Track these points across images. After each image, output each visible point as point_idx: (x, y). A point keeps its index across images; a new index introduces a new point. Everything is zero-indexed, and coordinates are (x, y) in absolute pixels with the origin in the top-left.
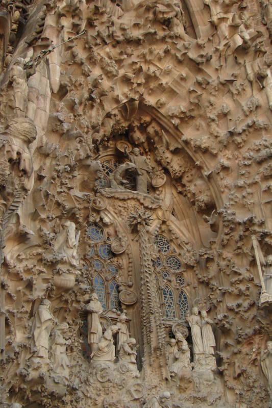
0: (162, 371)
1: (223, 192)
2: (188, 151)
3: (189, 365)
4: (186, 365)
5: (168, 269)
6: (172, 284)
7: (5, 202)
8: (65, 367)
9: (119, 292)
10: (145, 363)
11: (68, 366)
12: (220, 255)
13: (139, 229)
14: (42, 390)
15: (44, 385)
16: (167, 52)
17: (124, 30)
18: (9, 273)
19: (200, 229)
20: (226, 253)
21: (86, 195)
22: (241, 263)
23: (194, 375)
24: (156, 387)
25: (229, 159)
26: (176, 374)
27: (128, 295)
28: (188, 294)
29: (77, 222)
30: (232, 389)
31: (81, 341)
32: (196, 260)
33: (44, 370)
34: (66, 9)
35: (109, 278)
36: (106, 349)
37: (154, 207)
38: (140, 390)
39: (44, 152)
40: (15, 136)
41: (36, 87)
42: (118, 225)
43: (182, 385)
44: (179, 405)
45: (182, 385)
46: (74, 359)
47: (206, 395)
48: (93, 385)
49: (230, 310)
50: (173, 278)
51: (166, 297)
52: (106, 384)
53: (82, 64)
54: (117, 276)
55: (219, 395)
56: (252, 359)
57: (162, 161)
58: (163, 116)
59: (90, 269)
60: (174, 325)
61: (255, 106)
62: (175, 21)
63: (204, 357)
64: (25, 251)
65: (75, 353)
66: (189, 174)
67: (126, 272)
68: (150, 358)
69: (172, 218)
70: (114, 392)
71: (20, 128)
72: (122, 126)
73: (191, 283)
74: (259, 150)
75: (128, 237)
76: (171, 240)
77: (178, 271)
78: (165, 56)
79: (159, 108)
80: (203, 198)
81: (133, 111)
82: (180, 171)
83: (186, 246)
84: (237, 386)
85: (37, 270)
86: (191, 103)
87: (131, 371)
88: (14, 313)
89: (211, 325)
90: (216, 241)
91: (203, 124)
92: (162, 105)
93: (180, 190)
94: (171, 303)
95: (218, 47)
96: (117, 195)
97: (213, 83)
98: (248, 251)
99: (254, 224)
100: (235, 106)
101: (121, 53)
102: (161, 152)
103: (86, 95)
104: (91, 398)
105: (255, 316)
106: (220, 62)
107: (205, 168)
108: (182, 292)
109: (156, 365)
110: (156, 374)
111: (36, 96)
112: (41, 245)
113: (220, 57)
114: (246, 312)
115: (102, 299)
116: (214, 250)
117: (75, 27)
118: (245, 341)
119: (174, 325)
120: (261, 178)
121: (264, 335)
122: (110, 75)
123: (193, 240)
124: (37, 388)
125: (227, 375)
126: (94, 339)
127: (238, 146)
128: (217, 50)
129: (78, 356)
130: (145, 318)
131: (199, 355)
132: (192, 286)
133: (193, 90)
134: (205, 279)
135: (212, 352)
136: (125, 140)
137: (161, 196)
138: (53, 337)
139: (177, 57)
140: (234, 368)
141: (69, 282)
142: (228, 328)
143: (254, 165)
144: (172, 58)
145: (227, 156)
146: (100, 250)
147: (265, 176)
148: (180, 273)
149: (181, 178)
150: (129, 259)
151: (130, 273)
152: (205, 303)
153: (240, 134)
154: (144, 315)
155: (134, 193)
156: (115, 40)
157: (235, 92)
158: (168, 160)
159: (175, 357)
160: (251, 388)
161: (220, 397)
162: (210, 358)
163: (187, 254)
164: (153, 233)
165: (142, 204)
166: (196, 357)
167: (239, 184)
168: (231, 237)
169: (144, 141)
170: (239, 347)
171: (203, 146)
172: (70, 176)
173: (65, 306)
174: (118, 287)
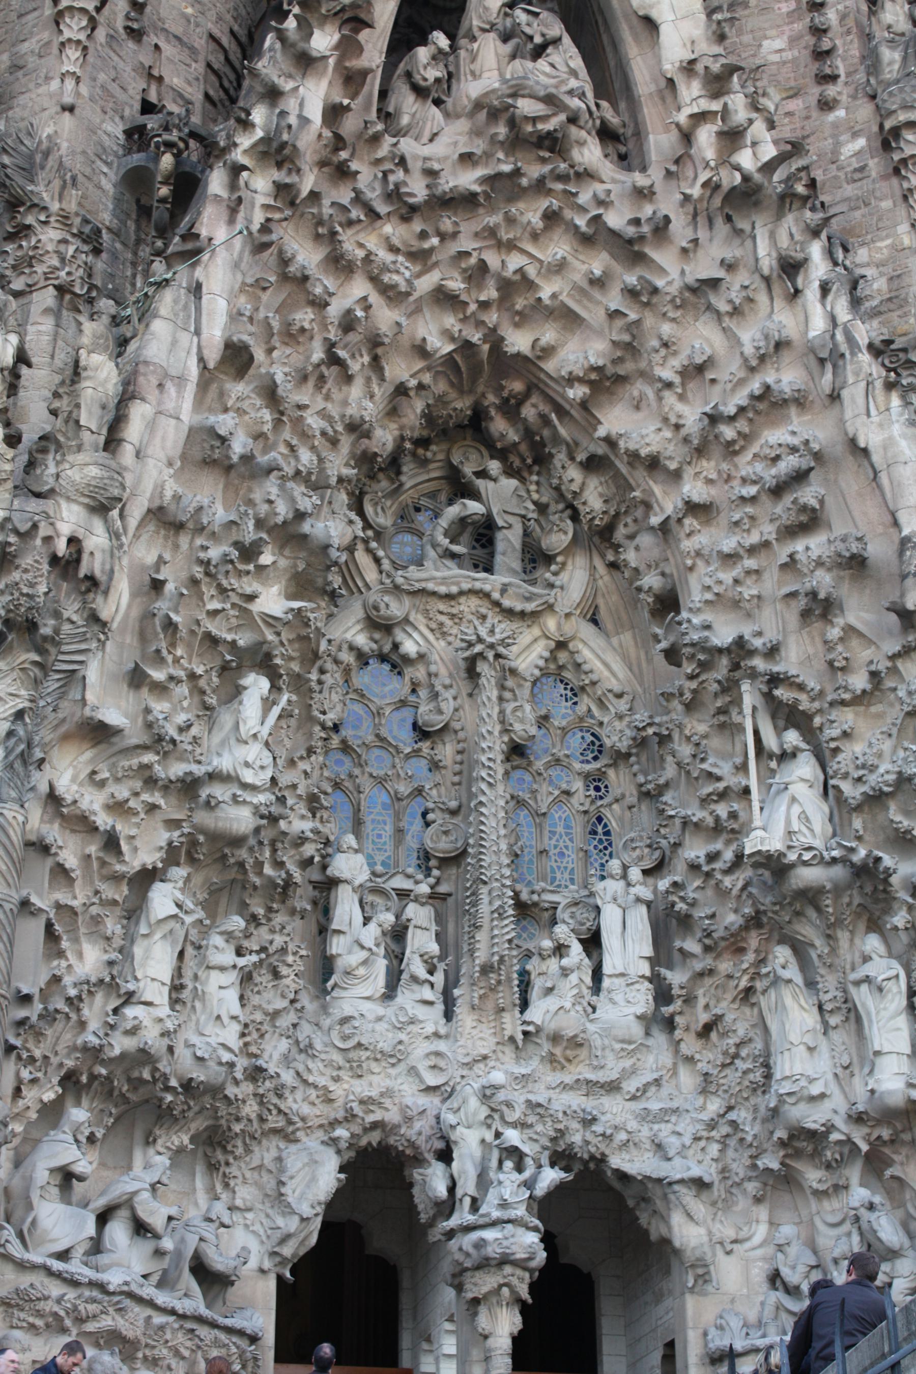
4: (568, 1005)
6: (575, 800)
7: (37, 658)
8: (226, 1020)
9: (428, 824)
11: (234, 1018)
12: (680, 726)
13: (478, 670)
14: (153, 1077)
16: (551, 217)
17: (431, 173)
18: (62, 815)
20: (695, 723)
21: (292, 610)
22: (729, 747)
23: (591, 1027)
24: (485, 1058)
25: (709, 482)
26: (539, 1030)
32: (634, 739)
34: (261, 148)
36: (361, 971)
37: (530, 607)
38: (442, 1064)
39: (171, 519)
40: (68, 499)
41: (156, 360)
42: (437, 658)
43: (558, 1051)
46: (283, 996)
48: (323, 1056)
49: (694, 867)
50: (578, 785)
52: (352, 1055)
53: (306, 278)
60: (564, 902)
61: (772, 343)
62: (575, 132)
64: (114, 759)
66: (629, 520)
69: (587, 630)
70: (376, 1070)
71: (77, 478)
72: (455, 409)
74: (776, 459)
76: (583, 689)
77: (588, 767)
78: (546, 228)
79: (539, 358)
80: (652, 581)
81: (476, 370)
82: (604, 513)
83: (614, 700)
86: (613, 342)
88: (71, 908)
89: (649, 907)
91: (650, 393)
92: (548, 351)
94: (566, 847)
95: (688, 191)
96: (430, 586)
97: (669, 289)
99: (752, 653)
100: (726, 343)
101: (423, 235)
103: (318, 355)
104: (316, 1087)
106: (695, 229)
108: (600, 819)
111: (155, 382)
113: (695, 215)
114: (728, 871)
117: (282, 190)
118: (723, 944)
120: (778, 532)
121: (771, 931)
122: (391, 294)
126: (337, 946)
128: (687, 198)
133: (617, 312)
134: (650, 786)
135: (646, 969)
136: (474, 440)
137: (562, 575)
139: (576, 227)
143: (764, 498)
144: (567, 230)
147: (786, 527)
153: (732, 419)
156: (405, 203)
157: (724, 307)
158: (575, 487)
161: (656, 1080)
162: (637, 986)
163: (618, 725)
164: (527, 675)
165: (497, 604)
166: (606, 983)
169: (517, 439)
172: (251, 567)
173: (240, 877)
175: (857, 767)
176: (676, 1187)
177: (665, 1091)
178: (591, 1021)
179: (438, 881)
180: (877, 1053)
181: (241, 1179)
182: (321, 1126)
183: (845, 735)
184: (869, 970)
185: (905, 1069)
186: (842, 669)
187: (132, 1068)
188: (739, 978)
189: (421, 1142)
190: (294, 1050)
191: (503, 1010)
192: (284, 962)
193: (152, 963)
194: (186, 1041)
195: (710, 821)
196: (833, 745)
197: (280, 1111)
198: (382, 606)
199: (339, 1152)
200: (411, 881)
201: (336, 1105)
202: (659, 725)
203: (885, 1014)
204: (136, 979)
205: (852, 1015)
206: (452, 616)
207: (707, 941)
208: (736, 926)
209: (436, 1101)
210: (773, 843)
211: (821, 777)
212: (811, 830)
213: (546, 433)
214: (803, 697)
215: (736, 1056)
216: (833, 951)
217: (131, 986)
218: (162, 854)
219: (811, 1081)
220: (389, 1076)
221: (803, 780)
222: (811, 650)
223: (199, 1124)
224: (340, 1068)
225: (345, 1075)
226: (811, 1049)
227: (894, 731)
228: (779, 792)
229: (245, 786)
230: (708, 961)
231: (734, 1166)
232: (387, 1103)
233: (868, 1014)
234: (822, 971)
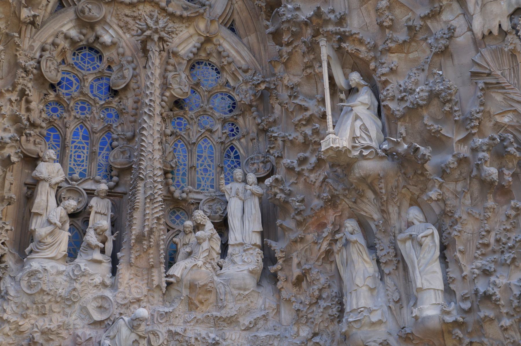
4: (200, 263)
6: (215, 136)
20: (291, 77)
24: (139, 300)
26: (179, 281)
28: (242, 151)
30: (288, 301)
31: (8, 227)
35: (98, 126)
36: (49, 240)
37: (185, 14)
38: (106, 305)
42: (124, 45)
44: (179, 330)
45: (193, 298)
47: (236, 313)
49: (290, 169)
52: (38, 298)
54: (114, 125)
55: (263, 313)
56: (322, 251)
63: (242, 250)
68: (131, 253)
69: (225, 32)
83: (244, 75)
84: (298, 296)
87: (91, 275)
89: (260, 198)
94: (209, 166)
99: (327, 22)
104: (9, 322)
108: (232, 148)
109: (142, 263)
110: (143, 280)
114: (311, 171)
115: (83, 161)
142: (282, 200)
146: (92, 87)
148: (232, 117)
161: (264, 316)
162: (251, 251)
163: (244, 87)
165: (163, 10)
166: (230, 250)
175: (401, 92)
177: (270, 324)
178: (218, 276)
179: (117, 184)
180: (420, 290)
183: (392, 71)
184: (412, 231)
186: (390, 27)
188: (321, 244)
191: (152, 267)
195: (301, 139)
196: (383, 78)
198: (87, 10)
201: (25, 335)
202: (269, 82)
205: (401, 265)
206: (134, 18)
207: (298, 218)
208: (319, 207)
209: (101, 331)
211: (376, 103)
212: (369, 137)
214: (363, 49)
215: (320, 298)
216: (386, 222)
219: (371, 311)
220: (66, 315)
221: (363, 104)
226: (371, 290)
227: (426, 67)
228: (346, 113)
230: (299, 233)
232: (64, 333)
233: (412, 262)
234: (378, 236)
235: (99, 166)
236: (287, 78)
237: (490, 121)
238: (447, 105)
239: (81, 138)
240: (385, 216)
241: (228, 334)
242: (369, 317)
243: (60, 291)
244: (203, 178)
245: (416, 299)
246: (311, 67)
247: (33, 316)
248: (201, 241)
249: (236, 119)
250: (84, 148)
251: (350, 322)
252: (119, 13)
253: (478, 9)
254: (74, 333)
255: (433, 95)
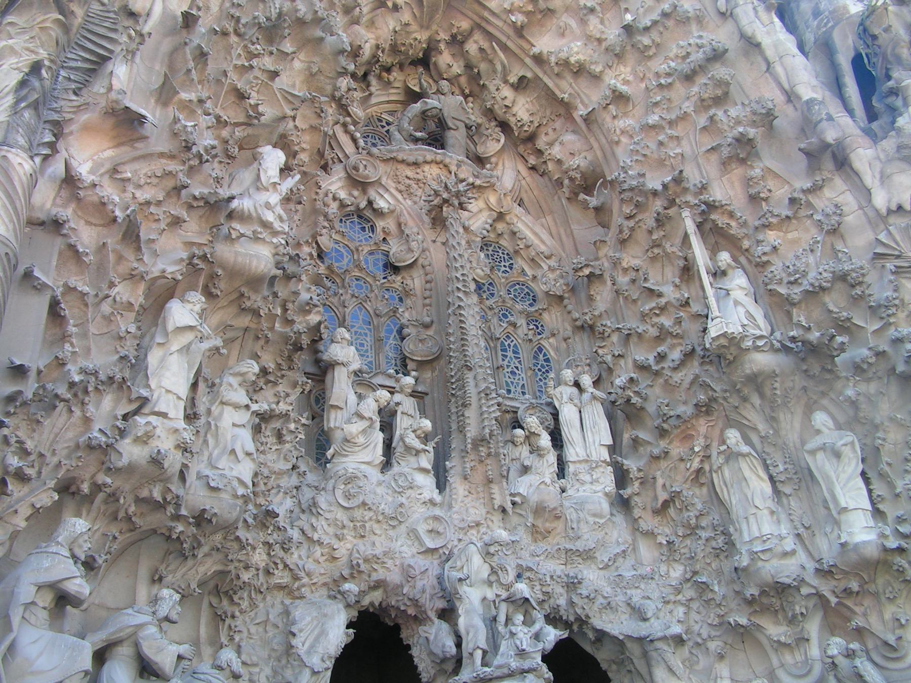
0: (493, 491)
1: (617, 143)
2: (546, 79)
3: (553, 482)
4: (548, 481)
5: (509, 303)
8: (241, 455)
9: (403, 339)
10: (452, 472)
11: (248, 454)
12: (616, 263)
13: (445, 214)
14: (165, 499)
15: (169, 486)
18: (79, 200)
19: (575, 232)
20: (630, 259)
23: (566, 504)
24: (478, 524)
27: (421, 341)
28: (552, 353)
29: (291, 154)
30: (650, 535)
31: (304, 421)
33: (165, 443)
36: (361, 440)
38: (441, 529)
42: (405, 212)
43: (539, 523)
44: (531, 565)
45: (540, 525)
49: (643, 368)
50: (522, 322)
51: (506, 356)
52: (358, 514)
54: (401, 310)
56: (692, 469)
57: (496, 107)
58: (493, 14)
59: (341, 291)
60: (522, 407)
65: (287, 446)
67: (420, 302)
69: (518, 210)
70: (378, 532)
73: (559, 332)
75: (424, 235)
82: (531, 122)
83: (548, 261)
85: (165, 212)
87: (419, 487)
90: (607, 239)
91: (573, 23)
93: (534, 163)
94: (517, 368)
96: (400, 156)
98: (674, 249)
99: (686, 190)
102: (492, 88)
104: (320, 543)
105: (697, 377)
107: (580, 106)
108: (540, 349)
109: (478, 477)
112: (175, 152)
114: (675, 369)
115: (367, 351)
116: (604, 260)
118: (676, 432)
119: (522, 407)
123: (561, 251)
124: (151, 491)
125: (640, 505)
126: (334, 420)
127: (644, 54)
129: (295, 453)
130: (453, 381)
131: (578, 465)
132: (560, 337)
135: (605, 455)
138: (215, 389)
140: (655, 490)
141: (254, 263)
142: (639, 405)
143: (678, 85)
145: (623, 76)
146: (367, 262)
148: (536, 311)
149: (531, 138)
150: (426, 275)
151: (427, 301)
152: (589, 365)
153: (646, 29)
154: (453, 374)
155: (436, 153)
158: (507, 103)
159: (523, 465)
160: (692, 531)
161: (624, 551)
162: (601, 469)
163: (551, 276)
166: (571, 468)
167: (650, 122)
168: (637, 223)
170: (663, 444)
171: (572, 60)
173: (253, 326)
174: (400, 331)
175: (790, 275)
176: (659, 645)
180: (845, 509)
181: (245, 634)
182: (325, 584)
185: (871, 523)
186: (766, 200)
187: (141, 486)
189: (425, 600)
190: (297, 510)
192: (287, 428)
193: (168, 374)
194: (198, 473)
196: (765, 259)
197: (286, 566)
198: (361, 168)
199: (348, 606)
200: (393, 380)
203: (843, 477)
204: (148, 386)
210: (734, 329)
213: (483, 66)
214: (733, 224)
215: (698, 527)
216: (777, 432)
217: (144, 393)
218: (182, 267)
221: (741, 288)
222: (731, 193)
223: (208, 567)
224: (344, 527)
225: (349, 535)
226: (772, 513)
229: (266, 225)
231: (696, 628)
232: (389, 564)
233: (827, 478)
235: (387, 358)
236: (626, 260)
237: (903, 311)
238: (858, 287)
239: (361, 322)
240: (775, 425)
241: (585, 572)
242: (782, 546)
243: (383, 506)
244: (512, 383)
245: (837, 523)
246: (658, 246)
247: (349, 537)
248: (546, 452)
249: (541, 314)
250: (366, 335)
251: (756, 553)
252: (398, 173)
253: (877, 182)
254: (402, 565)
255: (842, 277)
